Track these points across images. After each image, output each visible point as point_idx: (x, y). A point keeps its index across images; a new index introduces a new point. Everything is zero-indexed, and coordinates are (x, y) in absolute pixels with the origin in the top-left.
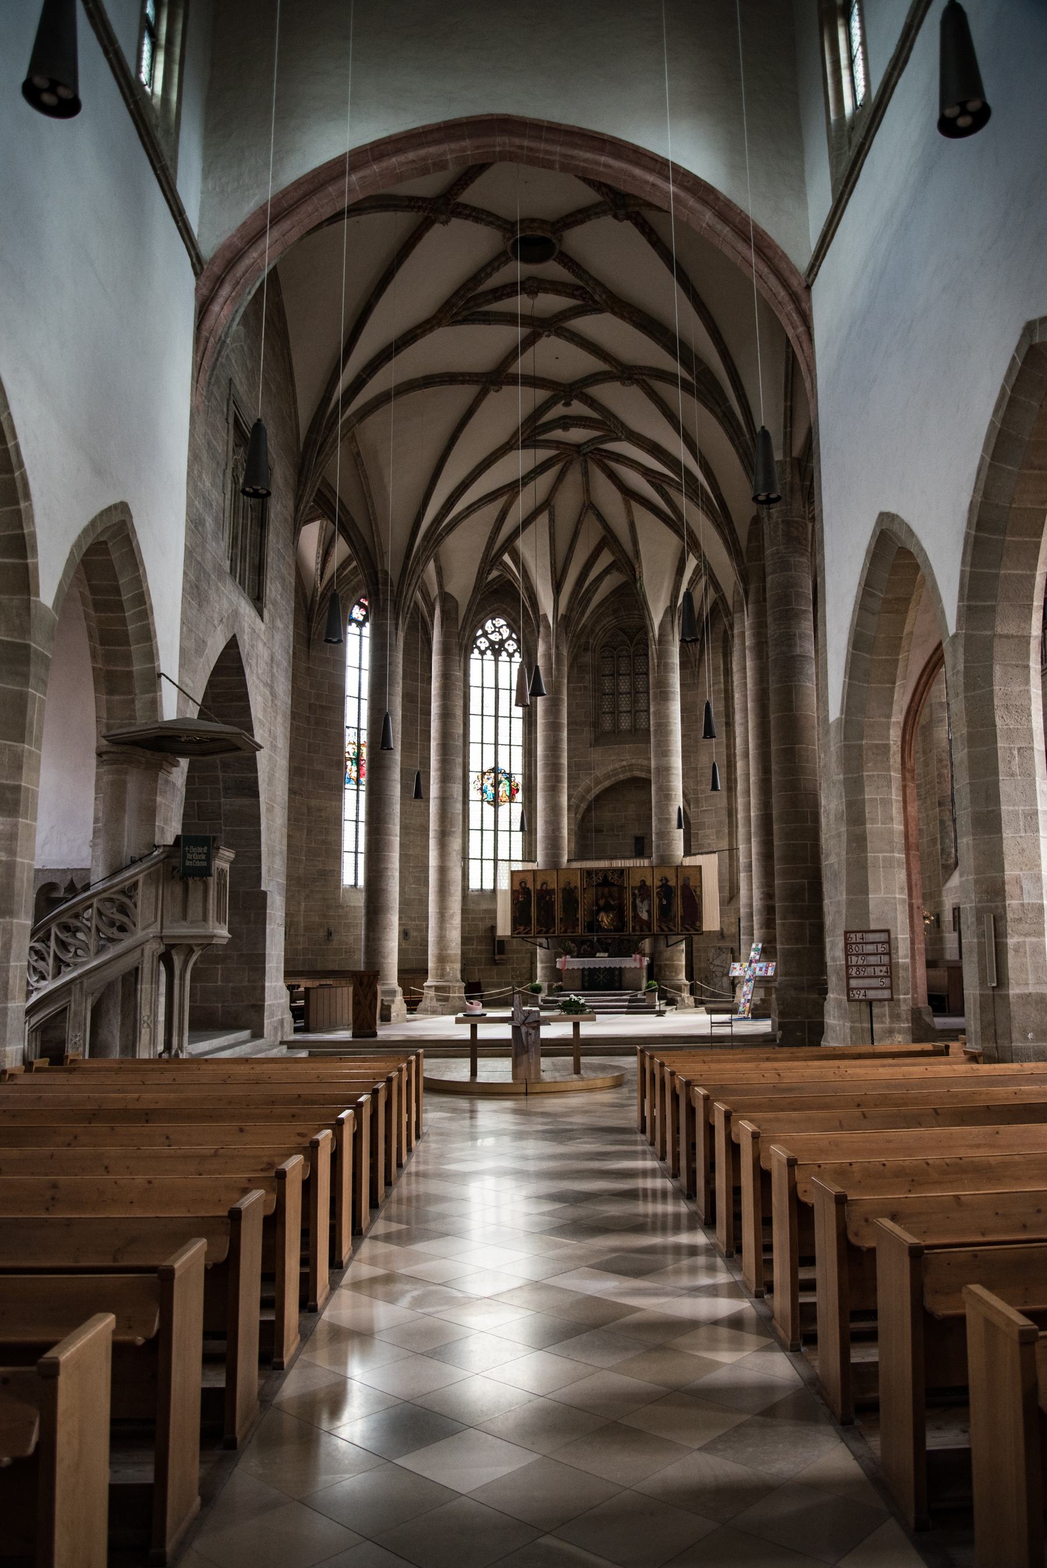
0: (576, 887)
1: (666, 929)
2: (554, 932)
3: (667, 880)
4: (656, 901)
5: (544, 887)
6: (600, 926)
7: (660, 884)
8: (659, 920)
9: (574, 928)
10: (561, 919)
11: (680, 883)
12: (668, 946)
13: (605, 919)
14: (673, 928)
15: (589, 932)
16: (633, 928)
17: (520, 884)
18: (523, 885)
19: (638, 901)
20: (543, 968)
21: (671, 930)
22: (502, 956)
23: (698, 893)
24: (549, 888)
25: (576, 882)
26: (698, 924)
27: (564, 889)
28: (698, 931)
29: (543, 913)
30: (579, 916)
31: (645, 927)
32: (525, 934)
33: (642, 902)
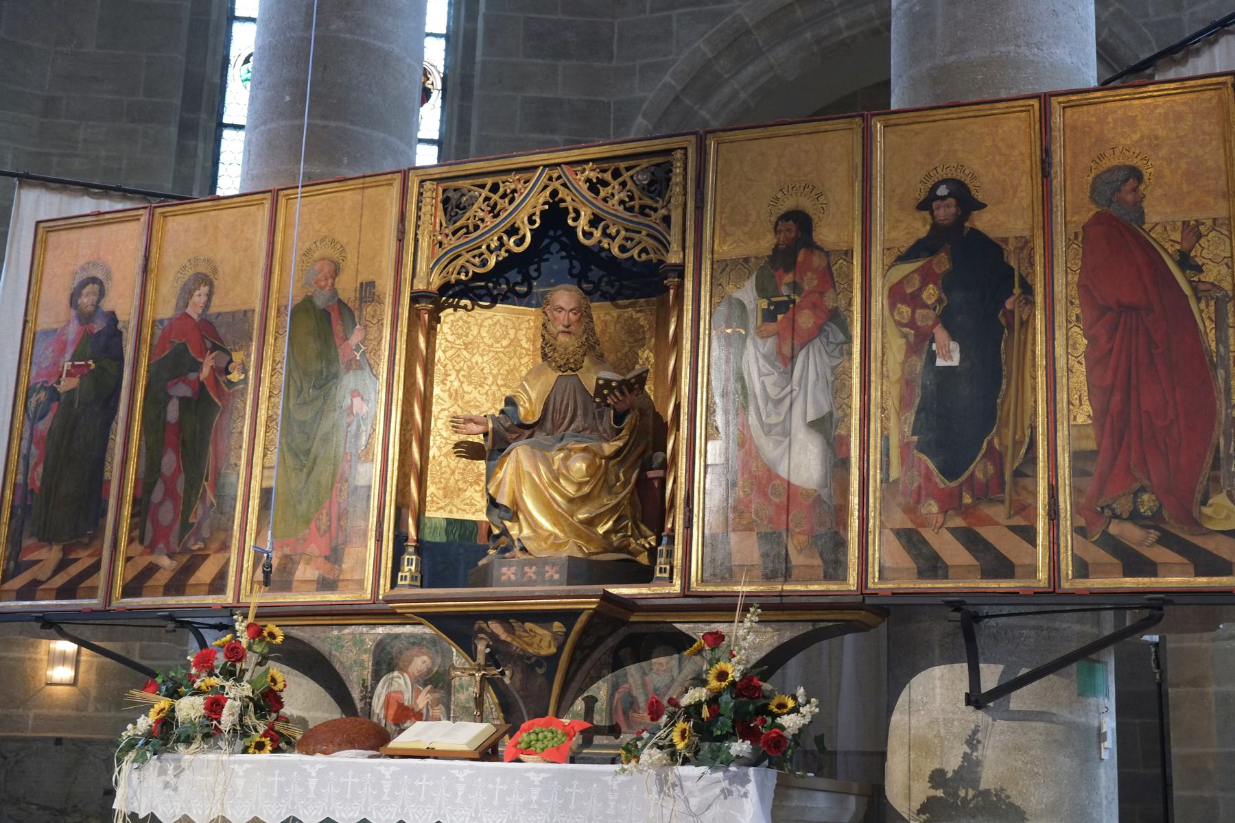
0: (368, 292)
1: (953, 552)
3: (966, 200)
7: (920, 227)
9: (334, 556)
14: (1007, 544)
17: (74, 300)
18: (86, 300)
24: (217, 306)
29: (169, 461)
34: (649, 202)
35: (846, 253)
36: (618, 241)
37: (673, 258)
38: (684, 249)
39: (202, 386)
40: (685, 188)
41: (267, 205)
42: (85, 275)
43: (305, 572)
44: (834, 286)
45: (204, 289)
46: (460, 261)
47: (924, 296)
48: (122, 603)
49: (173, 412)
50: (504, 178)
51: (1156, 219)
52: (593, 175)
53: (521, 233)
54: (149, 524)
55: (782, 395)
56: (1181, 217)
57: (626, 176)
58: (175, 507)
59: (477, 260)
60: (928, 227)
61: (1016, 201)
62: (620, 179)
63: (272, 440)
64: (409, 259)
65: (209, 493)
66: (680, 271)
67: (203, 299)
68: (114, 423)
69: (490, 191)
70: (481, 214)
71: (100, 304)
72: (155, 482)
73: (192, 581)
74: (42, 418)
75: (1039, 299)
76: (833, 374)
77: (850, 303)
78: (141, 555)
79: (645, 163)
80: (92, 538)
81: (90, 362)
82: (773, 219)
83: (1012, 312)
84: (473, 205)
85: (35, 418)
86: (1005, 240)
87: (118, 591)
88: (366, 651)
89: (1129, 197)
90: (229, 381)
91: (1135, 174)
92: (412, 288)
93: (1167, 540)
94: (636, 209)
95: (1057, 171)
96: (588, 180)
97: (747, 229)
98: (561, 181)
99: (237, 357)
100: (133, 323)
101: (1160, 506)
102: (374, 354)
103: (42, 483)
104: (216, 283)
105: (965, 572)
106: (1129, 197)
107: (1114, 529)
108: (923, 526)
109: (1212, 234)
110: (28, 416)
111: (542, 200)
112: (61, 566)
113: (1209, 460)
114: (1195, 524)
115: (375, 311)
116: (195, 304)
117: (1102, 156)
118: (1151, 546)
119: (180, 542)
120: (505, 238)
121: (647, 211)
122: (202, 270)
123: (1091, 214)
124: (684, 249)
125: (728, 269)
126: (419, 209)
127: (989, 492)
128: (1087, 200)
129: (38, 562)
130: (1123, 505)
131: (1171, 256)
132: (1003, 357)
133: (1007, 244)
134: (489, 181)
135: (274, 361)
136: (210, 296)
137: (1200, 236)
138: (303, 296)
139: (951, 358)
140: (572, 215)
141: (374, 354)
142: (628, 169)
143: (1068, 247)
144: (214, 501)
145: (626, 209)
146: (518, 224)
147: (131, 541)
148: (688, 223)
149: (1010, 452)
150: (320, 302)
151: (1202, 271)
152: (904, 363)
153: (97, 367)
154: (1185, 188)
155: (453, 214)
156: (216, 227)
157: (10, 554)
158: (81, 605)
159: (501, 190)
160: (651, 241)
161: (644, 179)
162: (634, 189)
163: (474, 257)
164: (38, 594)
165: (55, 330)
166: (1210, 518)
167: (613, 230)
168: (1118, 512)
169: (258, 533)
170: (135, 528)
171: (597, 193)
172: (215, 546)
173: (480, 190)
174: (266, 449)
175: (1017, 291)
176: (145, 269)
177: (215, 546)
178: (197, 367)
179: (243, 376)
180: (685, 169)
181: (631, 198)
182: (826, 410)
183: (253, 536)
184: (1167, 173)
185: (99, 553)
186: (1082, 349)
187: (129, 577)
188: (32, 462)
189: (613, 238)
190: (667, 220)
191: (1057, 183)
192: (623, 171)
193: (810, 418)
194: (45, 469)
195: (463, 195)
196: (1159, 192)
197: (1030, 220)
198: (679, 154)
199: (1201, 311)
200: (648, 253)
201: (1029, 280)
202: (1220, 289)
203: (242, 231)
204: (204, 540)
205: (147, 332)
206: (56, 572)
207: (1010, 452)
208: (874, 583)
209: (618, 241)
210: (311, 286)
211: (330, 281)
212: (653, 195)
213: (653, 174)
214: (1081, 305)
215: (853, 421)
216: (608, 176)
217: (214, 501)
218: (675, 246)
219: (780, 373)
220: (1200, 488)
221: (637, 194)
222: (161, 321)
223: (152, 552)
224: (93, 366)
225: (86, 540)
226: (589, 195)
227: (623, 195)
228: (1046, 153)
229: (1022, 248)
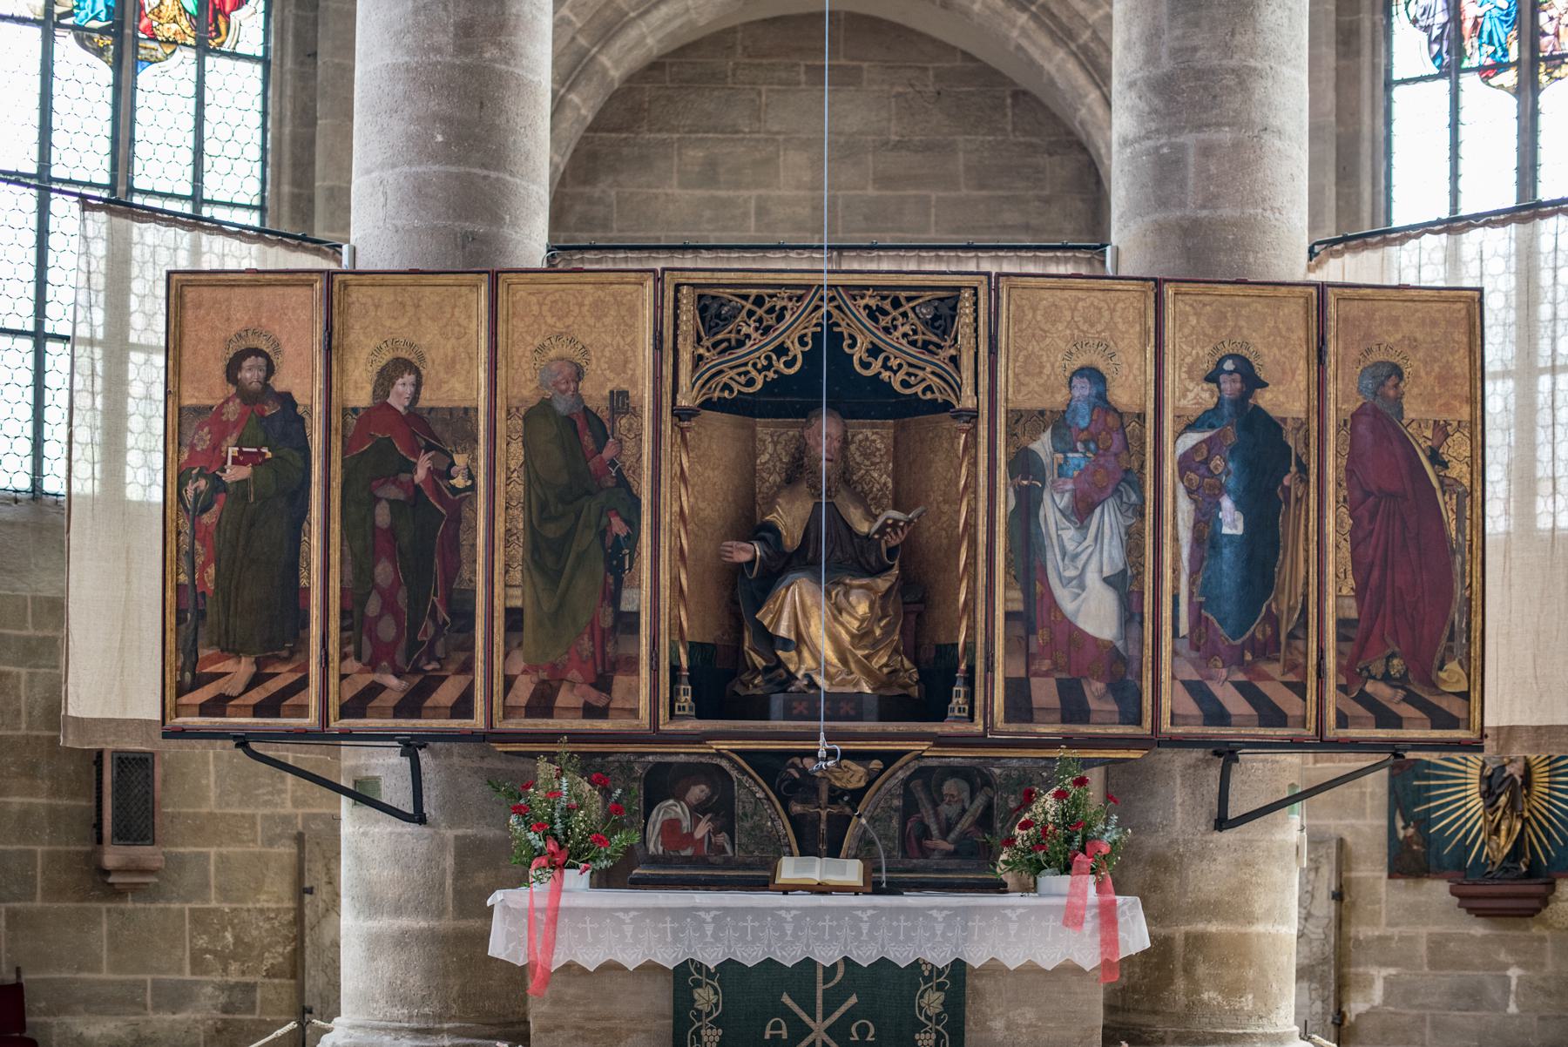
0: (621, 401)
1: (1236, 704)
2: (463, 707)
3: (1251, 380)
4: (1182, 512)
5: (399, 396)
6: (781, 679)
7: (1200, 397)
8: (1201, 643)
9: (603, 683)
10: (514, 618)
11: (1343, 397)
12: (1222, 822)
13: (817, 630)
15: (700, 715)
16: (1018, 692)
18: (250, 373)
19: (1052, 510)
20: (375, 943)
21: (1271, 715)
22: (142, 852)
23: (1458, 470)
24: (427, 399)
25: (623, 363)
26: (1452, 676)
27: (538, 415)
28: (1453, 723)
29: (384, 572)
30: (638, 598)
31: (1094, 690)
32: (259, 710)
33: (1081, 511)
34: (935, 339)
35: (1139, 416)
36: (901, 375)
37: (968, 402)
38: (976, 394)
39: (417, 488)
40: (976, 330)
41: (484, 289)
42: (243, 345)
43: (564, 698)
44: (1128, 449)
45: (409, 378)
46: (725, 379)
47: (1212, 465)
48: (336, 725)
49: (383, 515)
50: (771, 291)
51: (1412, 415)
52: (873, 303)
53: (791, 354)
54: (365, 638)
55: (1079, 549)
56: (1432, 417)
57: (907, 307)
58: (399, 624)
59: (743, 379)
60: (1215, 400)
61: (1294, 384)
62: (901, 310)
63: (514, 556)
64: (667, 370)
65: (440, 608)
66: (973, 415)
67: (409, 390)
69: (754, 303)
70: (745, 330)
72: (370, 593)
73: (428, 703)
74: (205, 509)
75: (1313, 479)
76: (1127, 533)
77: (1142, 466)
78: (360, 672)
79: (928, 295)
80: (292, 653)
81: (265, 450)
82: (1068, 374)
83: (1289, 488)
84: (735, 317)
85: (195, 511)
86: (1284, 420)
87: (334, 710)
88: (635, 779)
89: (1391, 393)
90: (453, 487)
91: (1397, 371)
92: (674, 403)
93: (1411, 699)
94: (919, 344)
95: (1331, 360)
96: (867, 307)
97: (1042, 381)
98: (835, 303)
99: (460, 460)
100: (318, 408)
101: (1407, 669)
102: (634, 472)
103: (217, 586)
104: (424, 372)
105: (1245, 722)
106: (1391, 393)
107: (1369, 687)
108: (1211, 678)
109: (1457, 435)
110: (185, 506)
111: (814, 321)
112: (255, 681)
113: (1447, 632)
114: (1433, 686)
115: (631, 425)
116: (399, 395)
117: (1369, 351)
118: (1398, 703)
119: (408, 661)
120: (774, 357)
121: (931, 347)
122: (403, 354)
123: (1359, 404)
124: (976, 394)
125: (1023, 420)
126: (676, 317)
127: (1267, 649)
128: (1355, 391)
130: (1378, 668)
131: (1424, 451)
132: (1281, 529)
133: (1285, 423)
134: (754, 292)
135: (508, 468)
136: (418, 385)
137: (1447, 436)
138: (539, 398)
139: (1236, 527)
140: (847, 342)
141: (634, 472)
142: (909, 299)
143: (1338, 432)
144: (448, 619)
145: (909, 343)
146: (789, 343)
147: (343, 657)
148: (981, 368)
149: (1285, 617)
150: (562, 407)
151: (1447, 468)
152: (1194, 526)
153: (275, 456)
154: (1437, 390)
155: (712, 324)
156: (417, 306)
158: (291, 725)
159: (767, 306)
160: (938, 380)
161: (927, 313)
162: (916, 321)
163: (739, 374)
165: (211, 408)
166: (1445, 681)
167: (894, 363)
168: (1373, 673)
169: (506, 655)
170: (349, 643)
171: (876, 321)
172: (452, 667)
173: (744, 303)
174: (507, 566)
175: (1293, 469)
176: (328, 348)
177: (452, 667)
178: (411, 468)
179: (469, 483)
180: (976, 311)
181: (915, 332)
182: (1121, 566)
183: (501, 658)
184: (1423, 373)
185: (305, 667)
186: (1348, 528)
187: (347, 696)
188: (199, 560)
189: (895, 372)
190: (954, 360)
191: (1331, 371)
192: (903, 301)
193: (1107, 572)
195: (722, 305)
196: (1415, 391)
197: (1305, 404)
198: (967, 294)
199: (1446, 503)
200: (933, 392)
201: (1304, 459)
202: (1462, 485)
203: (453, 315)
204: (439, 660)
205: (336, 420)
206: (250, 687)
207: (1285, 617)
208: (1166, 726)
209: (901, 375)
210: (547, 388)
211: (572, 386)
212: (938, 332)
213: (936, 308)
214: (1348, 488)
215: (1146, 579)
216: (887, 305)
217: (448, 619)
218: (968, 390)
219: (1078, 529)
220: (1438, 656)
221: (921, 328)
222: (355, 410)
223: (374, 670)
224: (269, 455)
225: (285, 653)
226: (868, 323)
227: (907, 329)
228: (1322, 340)
229: (1298, 430)
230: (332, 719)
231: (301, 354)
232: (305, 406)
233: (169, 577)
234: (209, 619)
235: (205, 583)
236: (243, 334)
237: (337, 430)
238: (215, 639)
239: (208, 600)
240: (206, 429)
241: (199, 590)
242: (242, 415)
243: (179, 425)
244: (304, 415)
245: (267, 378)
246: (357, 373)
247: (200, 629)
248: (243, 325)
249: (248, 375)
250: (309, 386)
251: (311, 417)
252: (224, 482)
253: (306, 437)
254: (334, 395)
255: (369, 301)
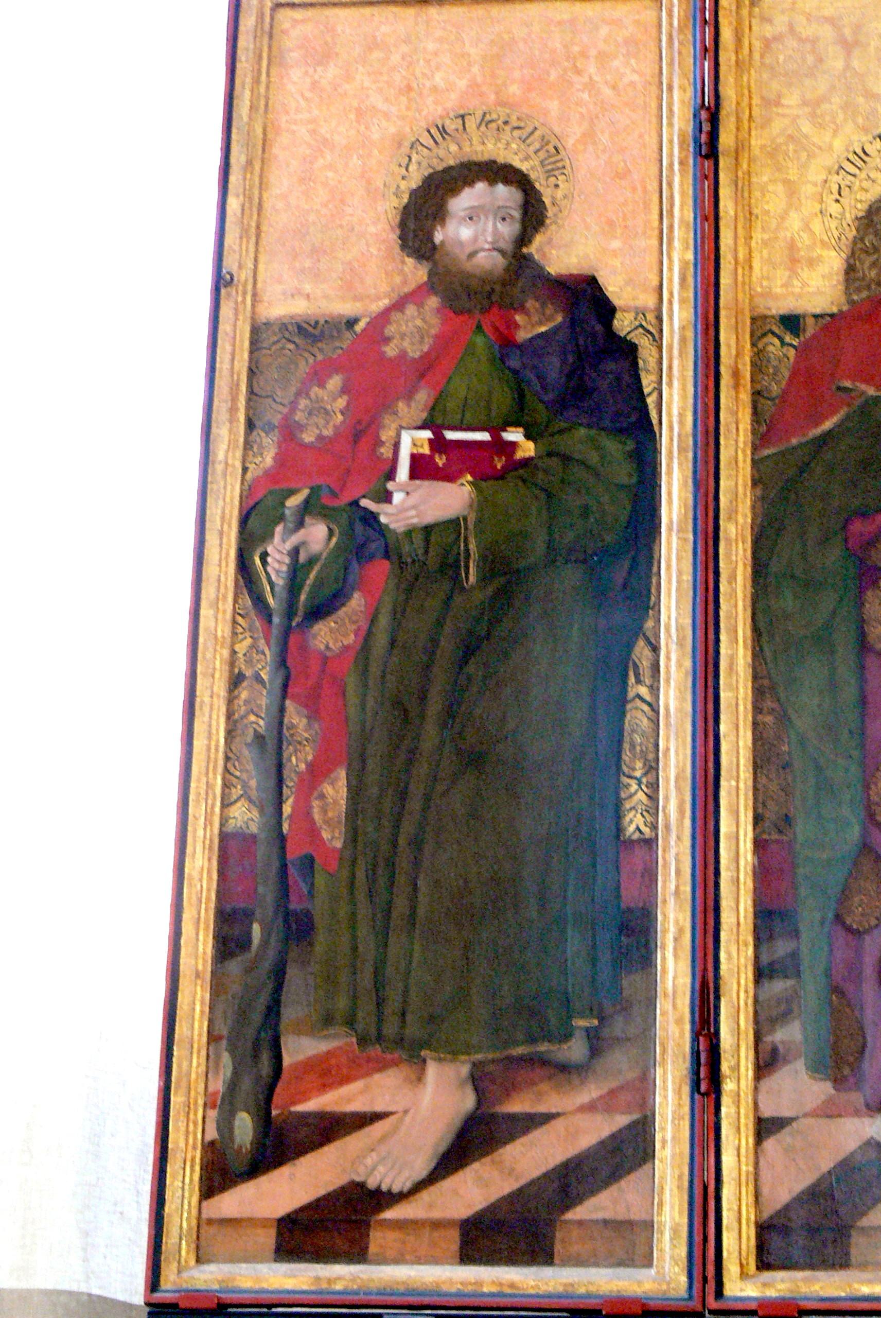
68: (641, 652)
71: (533, 249)
74: (318, 612)
78: (829, 1111)
81: (514, 435)
85: (290, 610)
103: (353, 835)
110: (259, 601)
129: (376, 1117)
157: (232, 1086)
164: (377, 1239)
165: (351, 323)
170: (784, 1017)
194: (356, 792)
222: (792, 322)
224: (527, 449)
230: (731, 1268)
231: (623, 175)
232: (641, 312)
233: (197, 810)
234: (321, 940)
235: (313, 832)
236: (451, 126)
237: (736, 374)
238: (342, 1003)
239: (320, 880)
240: (335, 382)
241: (293, 854)
242: (443, 343)
243: (252, 372)
244: (635, 338)
245: (523, 239)
246: (794, 222)
247: (293, 973)
248: (452, 101)
249: (466, 233)
250: (653, 258)
251: (657, 341)
252: (382, 530)
253: (642, 398)
254: (725, 280)
255: (827, 32)
